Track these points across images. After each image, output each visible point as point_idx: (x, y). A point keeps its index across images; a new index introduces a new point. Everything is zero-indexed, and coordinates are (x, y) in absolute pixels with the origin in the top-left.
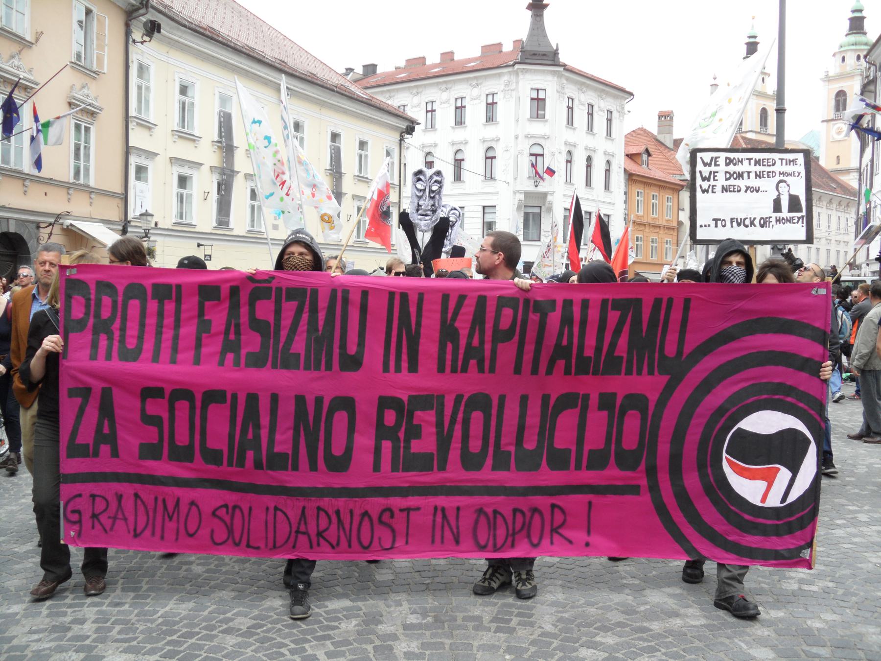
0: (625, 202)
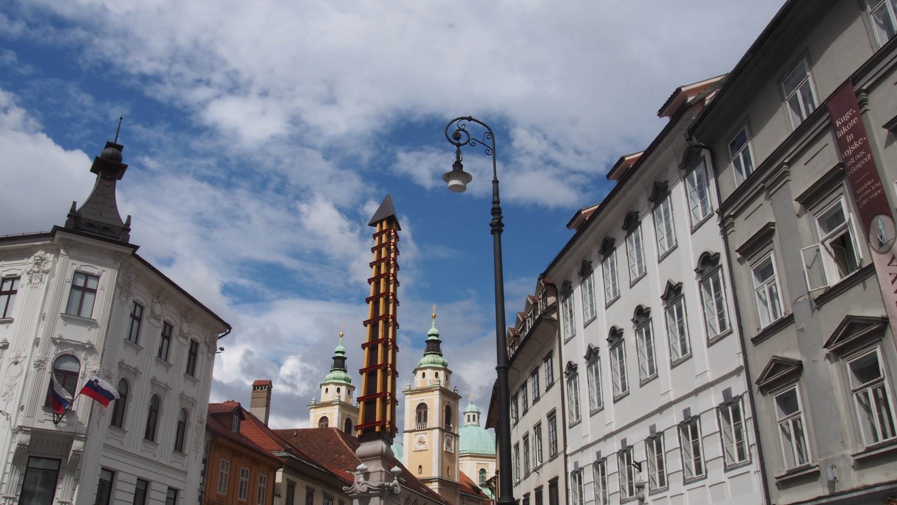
0: (203, 473)
